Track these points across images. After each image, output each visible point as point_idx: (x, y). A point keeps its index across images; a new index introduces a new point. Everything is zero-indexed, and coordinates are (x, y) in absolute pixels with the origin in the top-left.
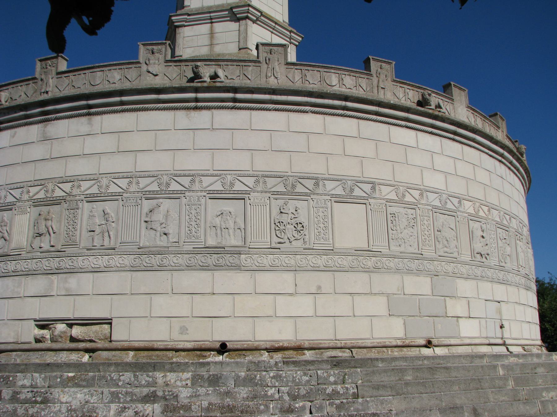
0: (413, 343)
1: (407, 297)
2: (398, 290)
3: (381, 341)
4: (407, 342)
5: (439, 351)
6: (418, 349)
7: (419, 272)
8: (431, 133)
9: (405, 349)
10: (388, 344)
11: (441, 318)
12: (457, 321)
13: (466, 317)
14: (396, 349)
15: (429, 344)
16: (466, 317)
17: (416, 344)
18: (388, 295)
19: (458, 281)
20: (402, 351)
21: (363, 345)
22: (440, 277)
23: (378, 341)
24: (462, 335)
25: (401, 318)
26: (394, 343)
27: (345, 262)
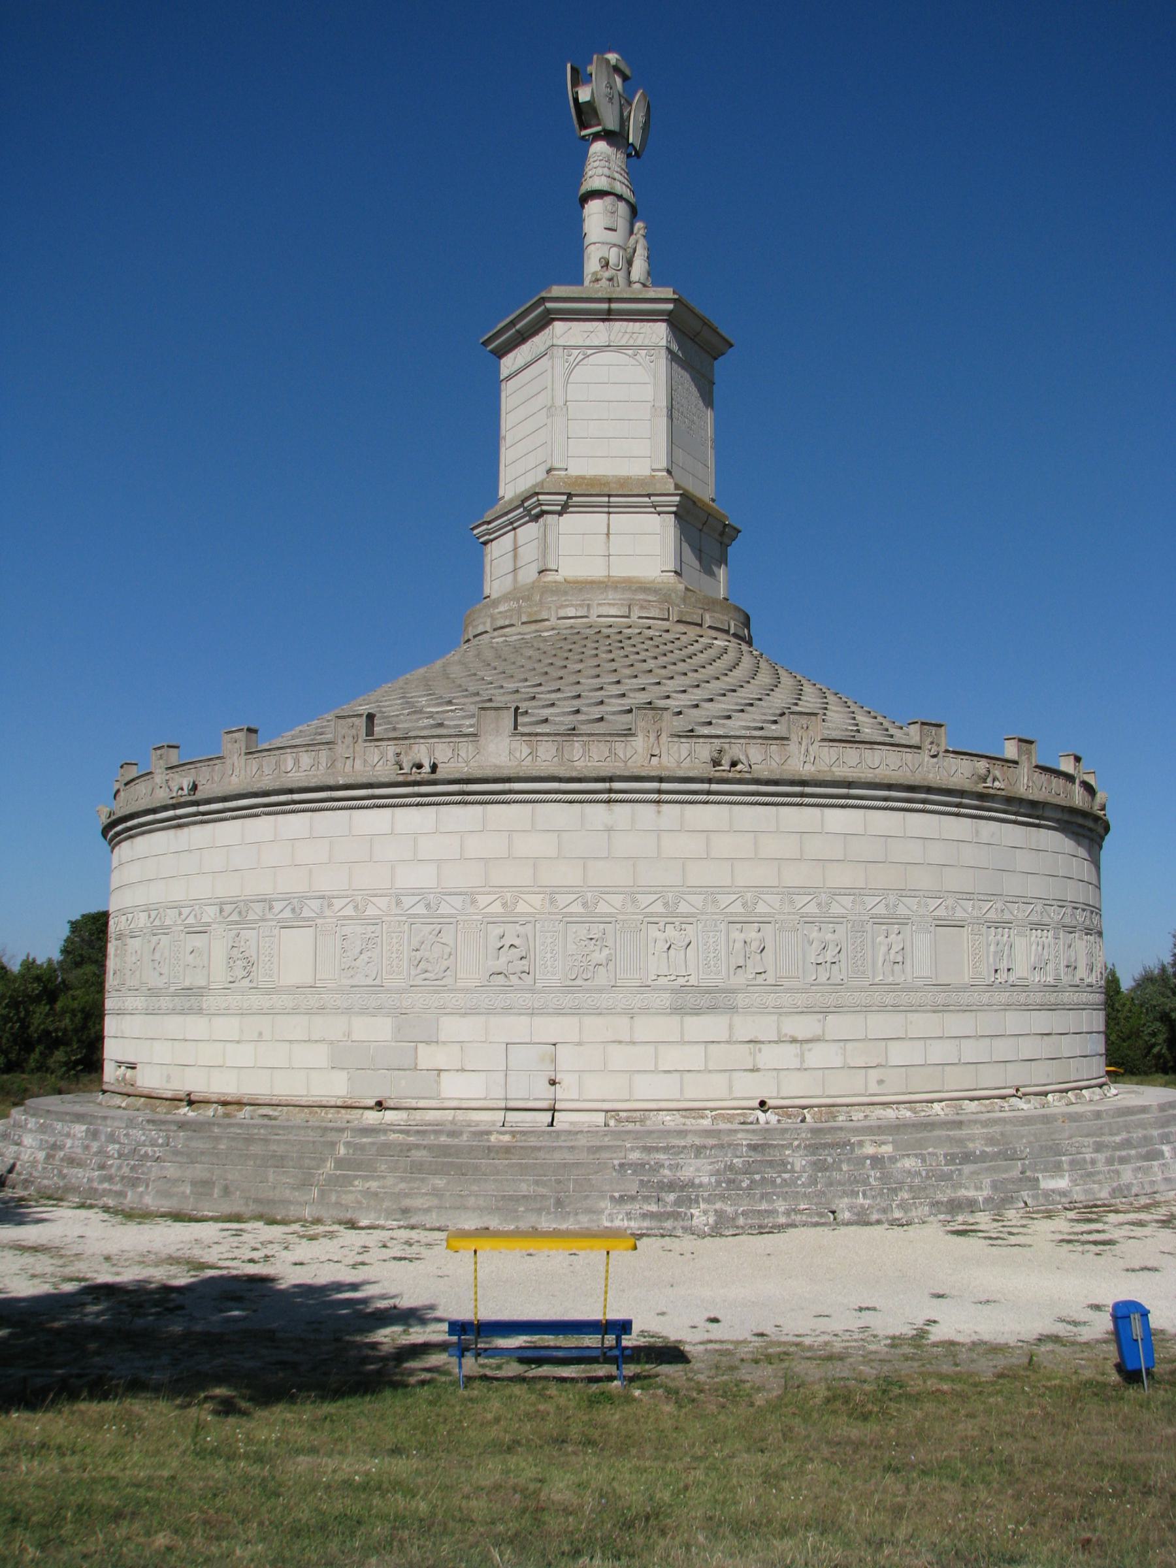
0: (357, 1104)
1: (356, 1044)
2: (344, 1035)
3: (318, 1099)
4: (349, 1102)
5: (390, 1116)
6: (361, 1111)
7: (377, 1011)
8: (418, 805)
9: (343, 1111)
10: (324, 1103)
11: (408, 1072)
12: (439, 1075)
13: (458, 1070)
14: (332, 1110)
15: (380, 1105)
16: (458, 1070)
17: (362, 1105)
18: (332, 1042)
19: (444, 1020)
20: (338, 1112)
21: (297, 1103)
22: (411, 1015)
23: (314, 1099)
24: (443, 1096)
25: (346, 1071)
26: (333, 1103)
27: (286, 1001)
